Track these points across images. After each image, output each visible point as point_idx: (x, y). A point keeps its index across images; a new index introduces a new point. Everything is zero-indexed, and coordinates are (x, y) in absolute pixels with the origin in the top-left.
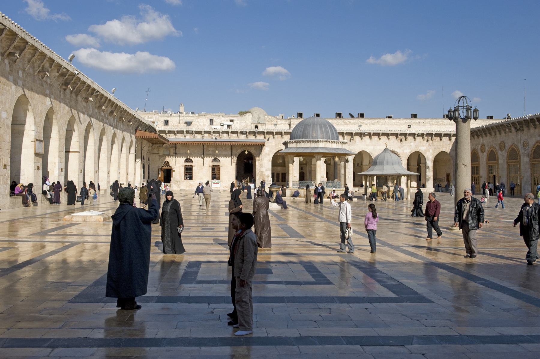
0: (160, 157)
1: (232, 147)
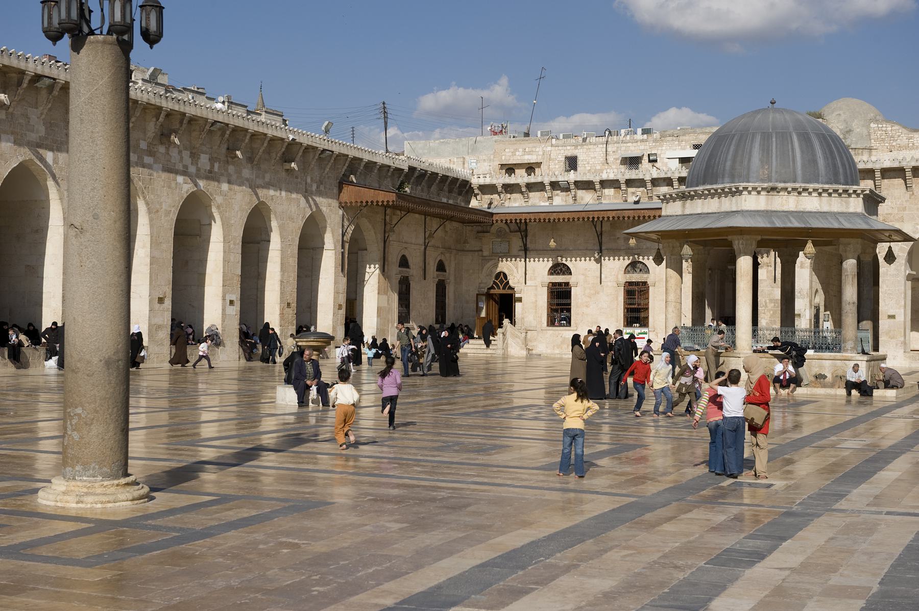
0: (485, 260)
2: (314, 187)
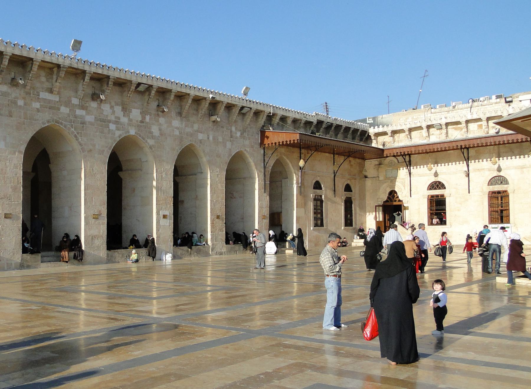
2: (239, 134)
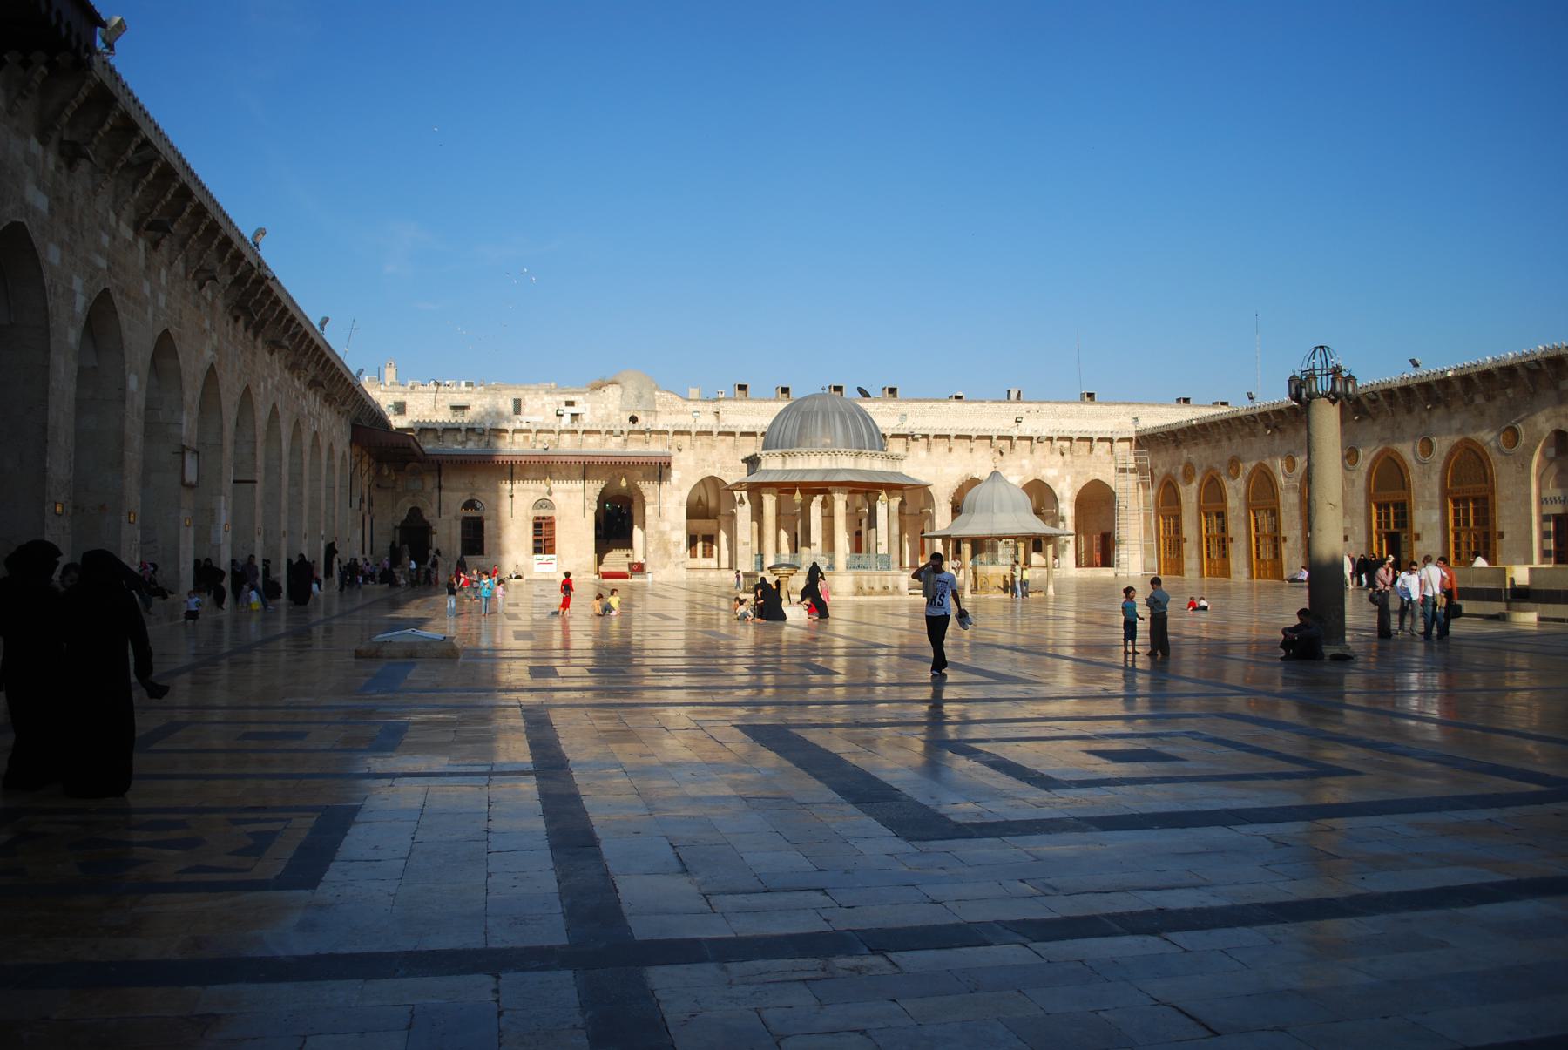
1: (585, 469)
